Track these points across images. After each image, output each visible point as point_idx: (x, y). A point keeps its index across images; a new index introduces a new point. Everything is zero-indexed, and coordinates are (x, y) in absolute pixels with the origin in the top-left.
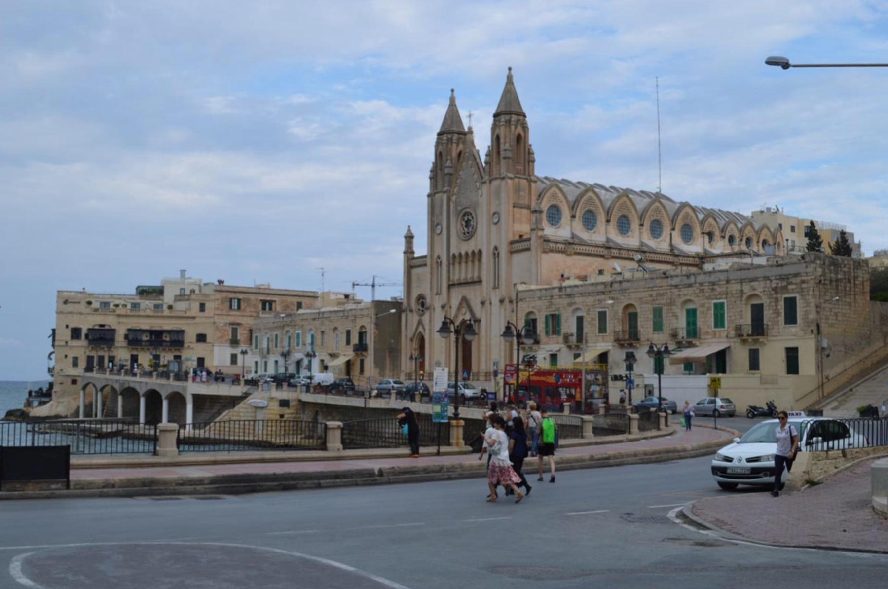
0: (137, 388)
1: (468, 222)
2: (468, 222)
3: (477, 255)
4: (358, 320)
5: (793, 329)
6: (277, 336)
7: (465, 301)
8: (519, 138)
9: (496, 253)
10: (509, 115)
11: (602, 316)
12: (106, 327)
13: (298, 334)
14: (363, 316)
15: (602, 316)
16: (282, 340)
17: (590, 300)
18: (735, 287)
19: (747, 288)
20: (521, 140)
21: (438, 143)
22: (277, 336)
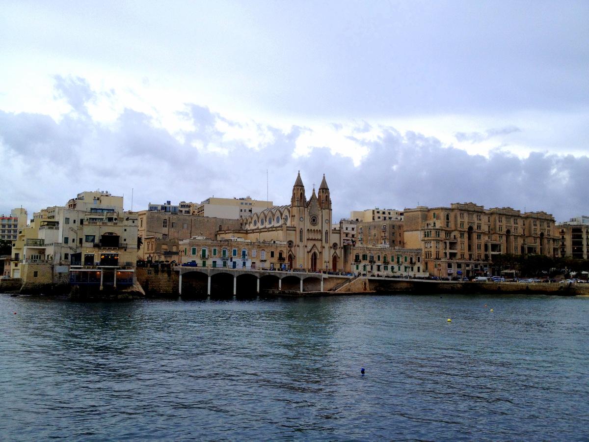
0: (278, 276)
1: (314, 220)
2: (314, 220)
3: (320, 232)
4: (278, 248)
5: (419, 263)
6: (215, 250)
7: (314, 245)
8: (327, 196)
9: (326, 233)
10: (324, 189)
11: (379, 257)
12: (114, 235)
13: (235, 251)
14: (281, 247)
15: (379, 257)
16: (220, 252)
17: (375, 252)
18: (409, 253)
19: (411, 254)
20: (327, 198)
21: (294, 190)
22: (215, 250)
